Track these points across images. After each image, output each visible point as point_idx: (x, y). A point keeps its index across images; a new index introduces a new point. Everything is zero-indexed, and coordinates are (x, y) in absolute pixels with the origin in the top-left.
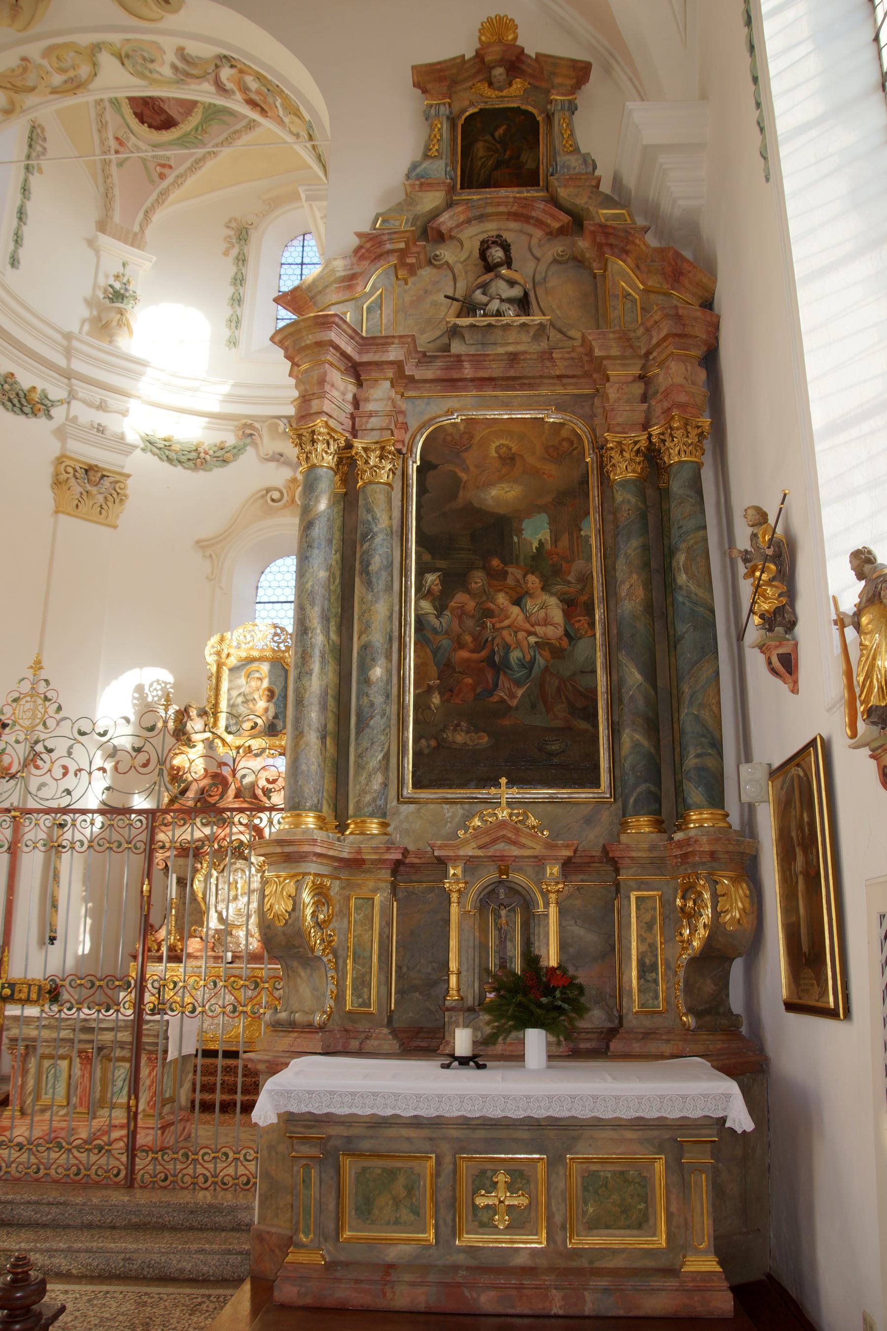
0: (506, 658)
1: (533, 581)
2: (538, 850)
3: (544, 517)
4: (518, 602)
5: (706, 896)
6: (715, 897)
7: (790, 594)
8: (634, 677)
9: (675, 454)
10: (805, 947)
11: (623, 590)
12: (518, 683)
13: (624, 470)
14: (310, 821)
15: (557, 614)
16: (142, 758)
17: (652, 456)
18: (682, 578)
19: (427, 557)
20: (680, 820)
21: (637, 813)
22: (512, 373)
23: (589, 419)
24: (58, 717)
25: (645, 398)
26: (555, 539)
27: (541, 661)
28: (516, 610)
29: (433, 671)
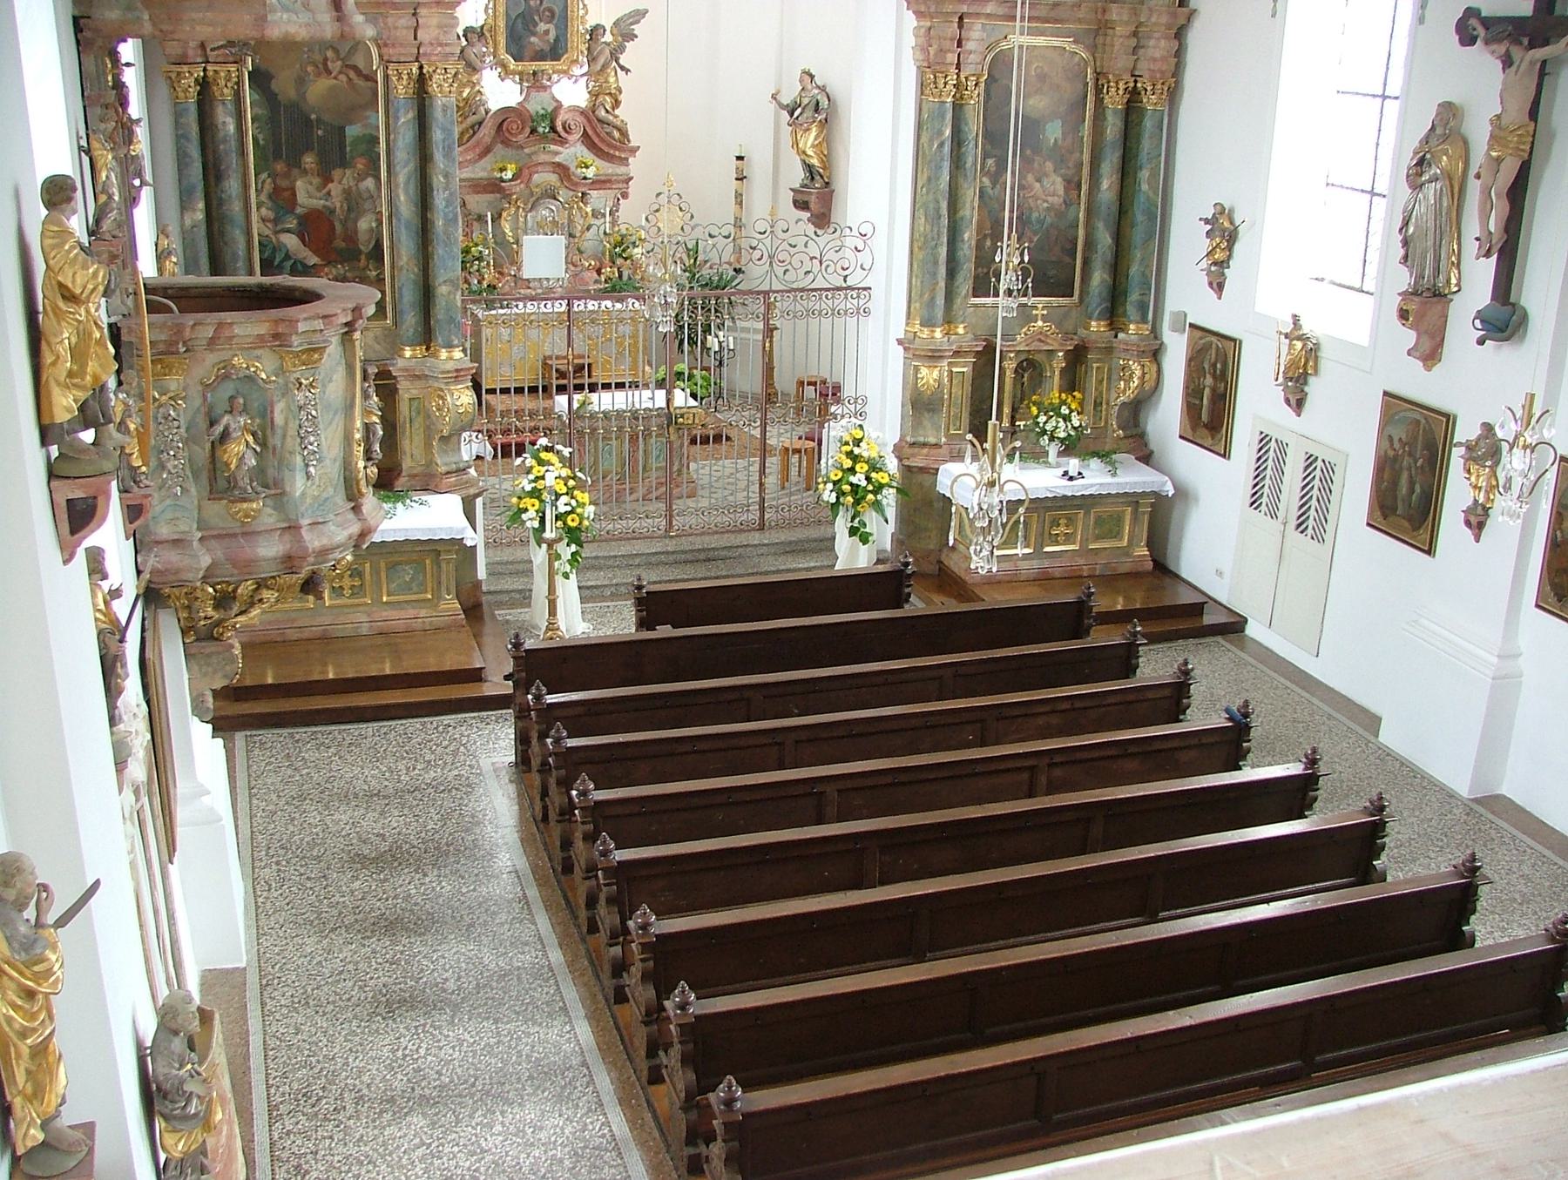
0: (1029, 217)
1: (1049, 166)
2: (1055, 346)
3: (1058, 123)
4: (1038, 180)
5: (1138, 373)
6: (1144, 374)
7: (1230, 257)
8: (1105, 239)
9: (1150, 101)
10: (1205, 417)
11: (1105, 185)
12: (1035, 233)
13: (1115, 101)
14: (938, 334)
15: (1060, 187)
16: (757, 254)
17: (1134, 95)
18: (1145, 187)
19: (988, 147)
20: (1125, 330)
21: (1098, 319)
22: (1052, 14)
23: (1093, 49)
24: (692, 223)
25: (1135, 50)
26: (1064, 139)
27: (1049, 220)
28: (1038, 185)
29: (988, 225)
